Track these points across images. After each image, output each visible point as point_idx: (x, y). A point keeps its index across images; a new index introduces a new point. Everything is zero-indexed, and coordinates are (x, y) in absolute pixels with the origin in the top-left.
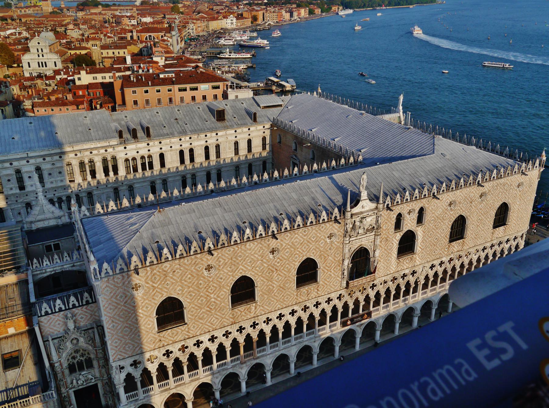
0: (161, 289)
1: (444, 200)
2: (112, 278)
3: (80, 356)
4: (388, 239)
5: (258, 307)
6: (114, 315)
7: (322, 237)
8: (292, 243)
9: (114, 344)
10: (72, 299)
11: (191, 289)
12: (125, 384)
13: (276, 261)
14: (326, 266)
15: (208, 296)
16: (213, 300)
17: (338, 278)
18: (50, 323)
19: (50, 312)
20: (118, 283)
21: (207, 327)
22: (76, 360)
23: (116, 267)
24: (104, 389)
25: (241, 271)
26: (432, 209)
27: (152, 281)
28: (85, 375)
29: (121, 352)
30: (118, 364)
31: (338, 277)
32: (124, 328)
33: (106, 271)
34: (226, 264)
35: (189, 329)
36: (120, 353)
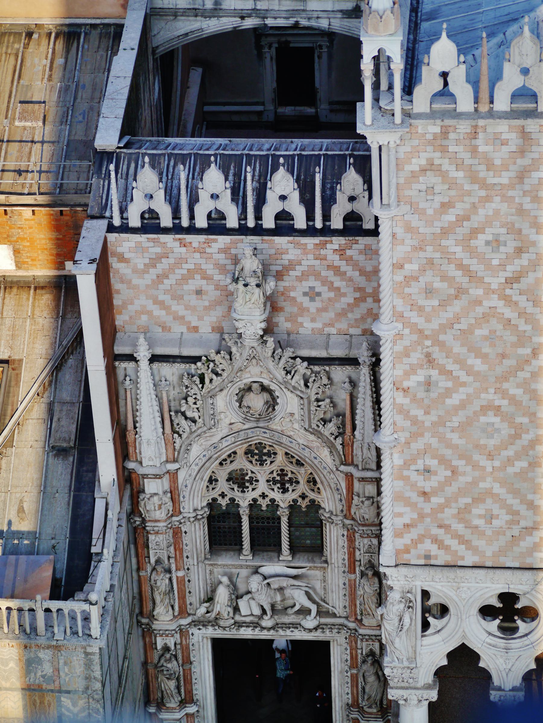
2: (464, 127)
3: (271, 481)
6: (443, 328)
9: (414, 477)
10: (283, 183)
12: (434, 695)
18: (161, 278)
19: (166, 221)
20: (490, 166)
22: (250, 495)
23: (497, 76)
24: (354, 679)
28: (276, 583)
29: (446, 527)
30: (419, 584)
32: (485, 409)
33: (439, 85)
36: (435, 531)
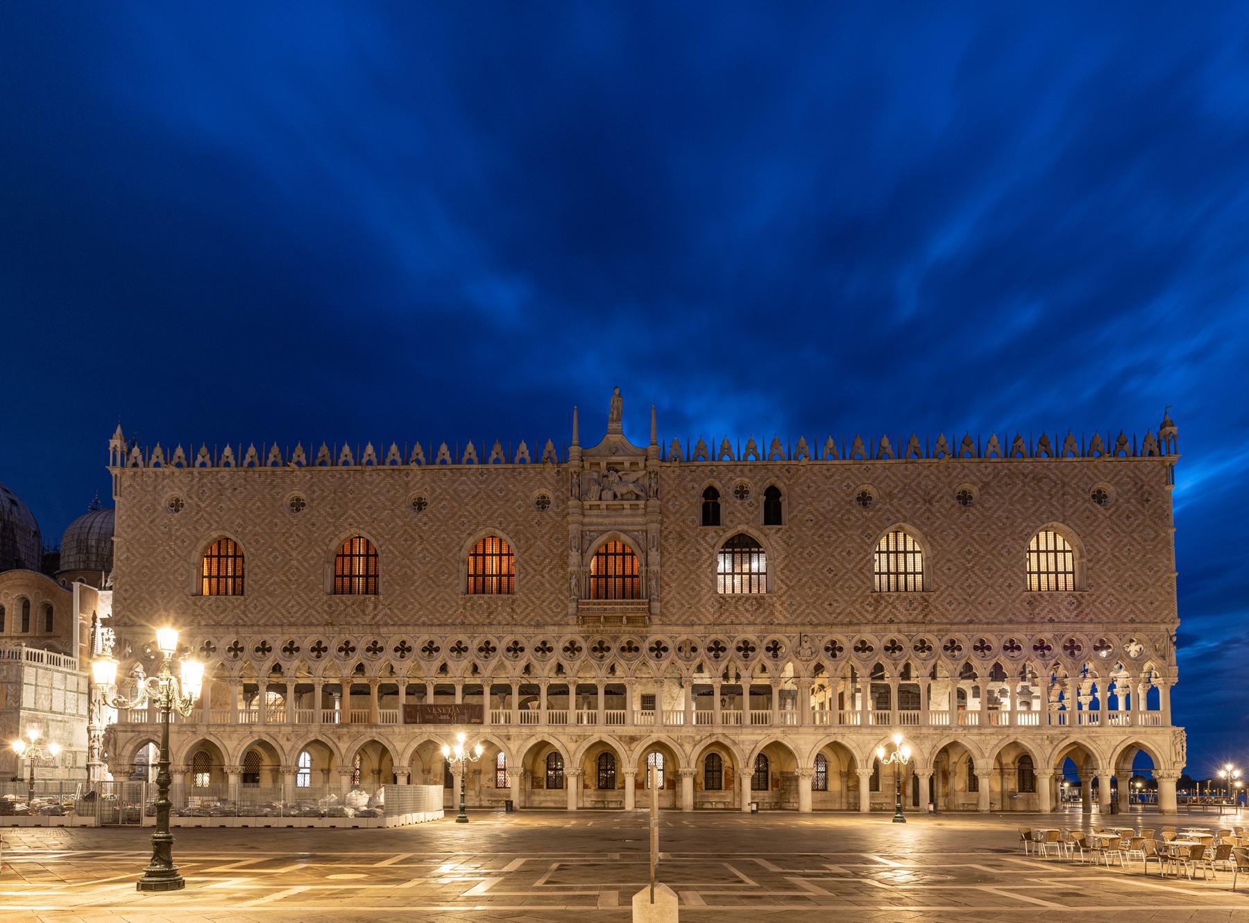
1: (837, 477)
4: (684, 535)
6: (133, 538)
8: (455, 490)
13: (420, 520)
16: (295, 562)
25: (351, 520)
26: (803, 492)
27: (198, 496)
31: (561, 593)
34: (324, 499)
35: (246, 606)
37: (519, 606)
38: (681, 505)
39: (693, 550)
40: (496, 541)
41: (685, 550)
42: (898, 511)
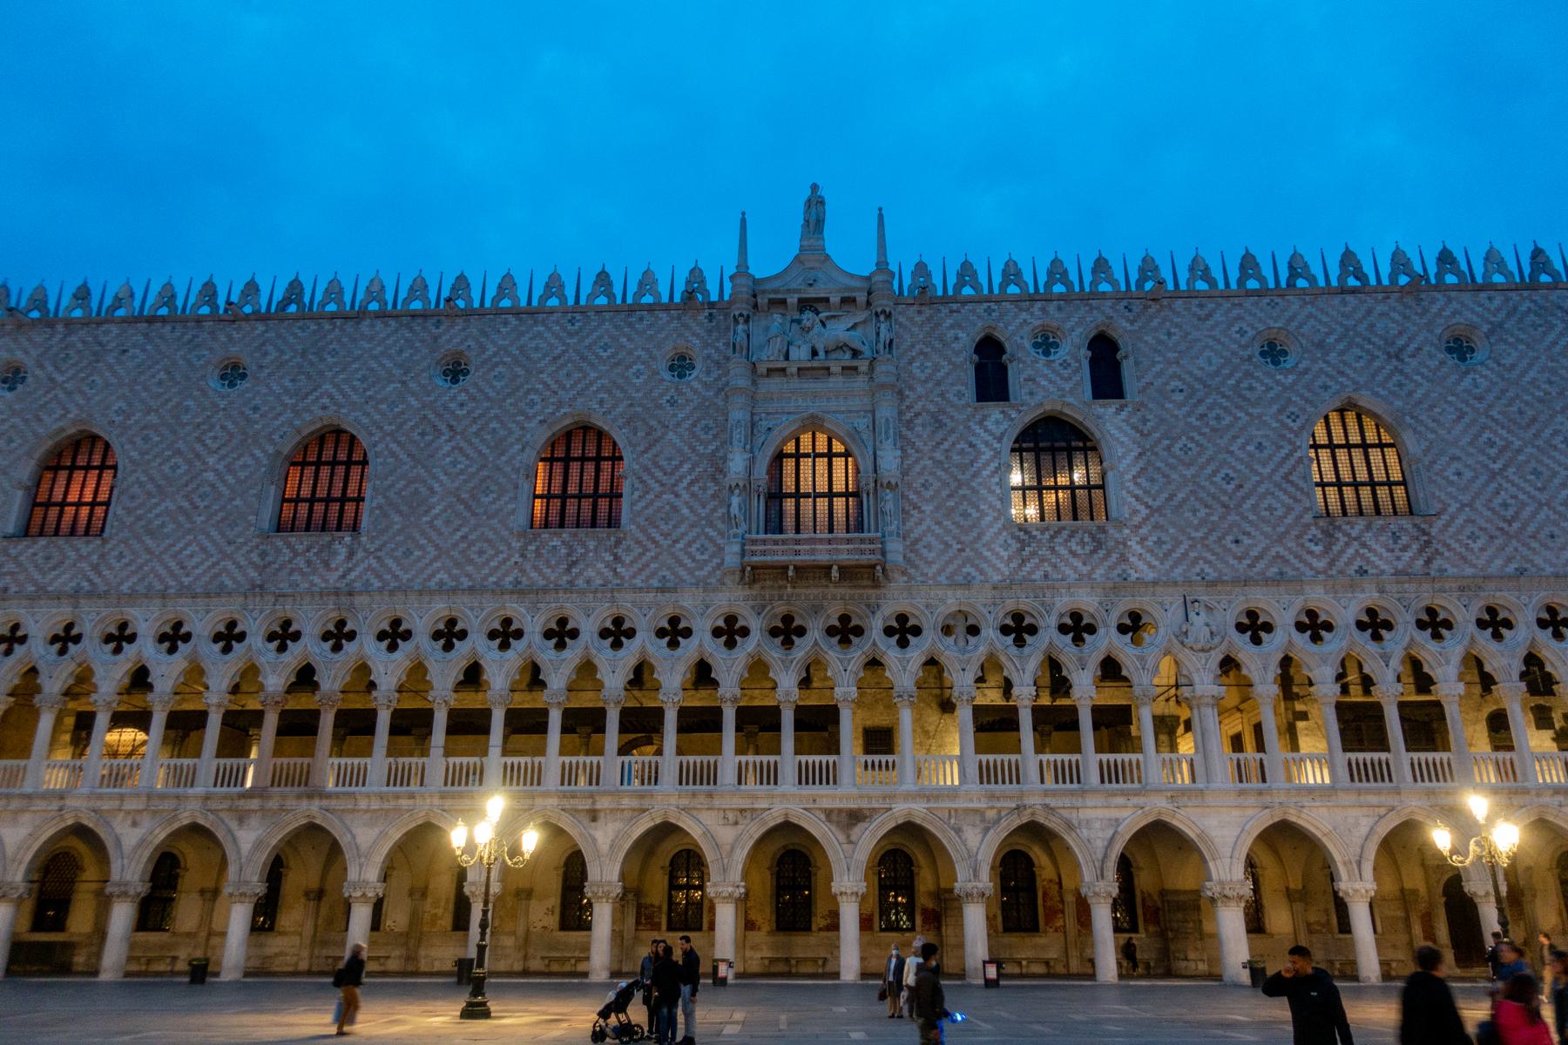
0: (69, 393)
1: (1218, 316)
5: (360, 554)
7: (639, 352)
8: (522, 349)
11: (153, 418)
13: (453, 399)
14: (656, 464)
15: (198, 456)
16: (210, 476)
17: (712, 533)
21: (163, 572)
26: (1160, 342)
31: (711, 525)
34: (282, 365)
35: (102, 556)
37: (628, 549)
38: (937, 369)
39: (962, 445)
40: (592, 437)
41: (946, 445)
42: (1342, 373)
